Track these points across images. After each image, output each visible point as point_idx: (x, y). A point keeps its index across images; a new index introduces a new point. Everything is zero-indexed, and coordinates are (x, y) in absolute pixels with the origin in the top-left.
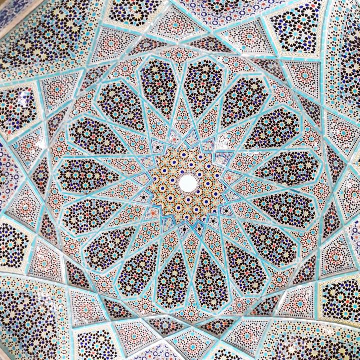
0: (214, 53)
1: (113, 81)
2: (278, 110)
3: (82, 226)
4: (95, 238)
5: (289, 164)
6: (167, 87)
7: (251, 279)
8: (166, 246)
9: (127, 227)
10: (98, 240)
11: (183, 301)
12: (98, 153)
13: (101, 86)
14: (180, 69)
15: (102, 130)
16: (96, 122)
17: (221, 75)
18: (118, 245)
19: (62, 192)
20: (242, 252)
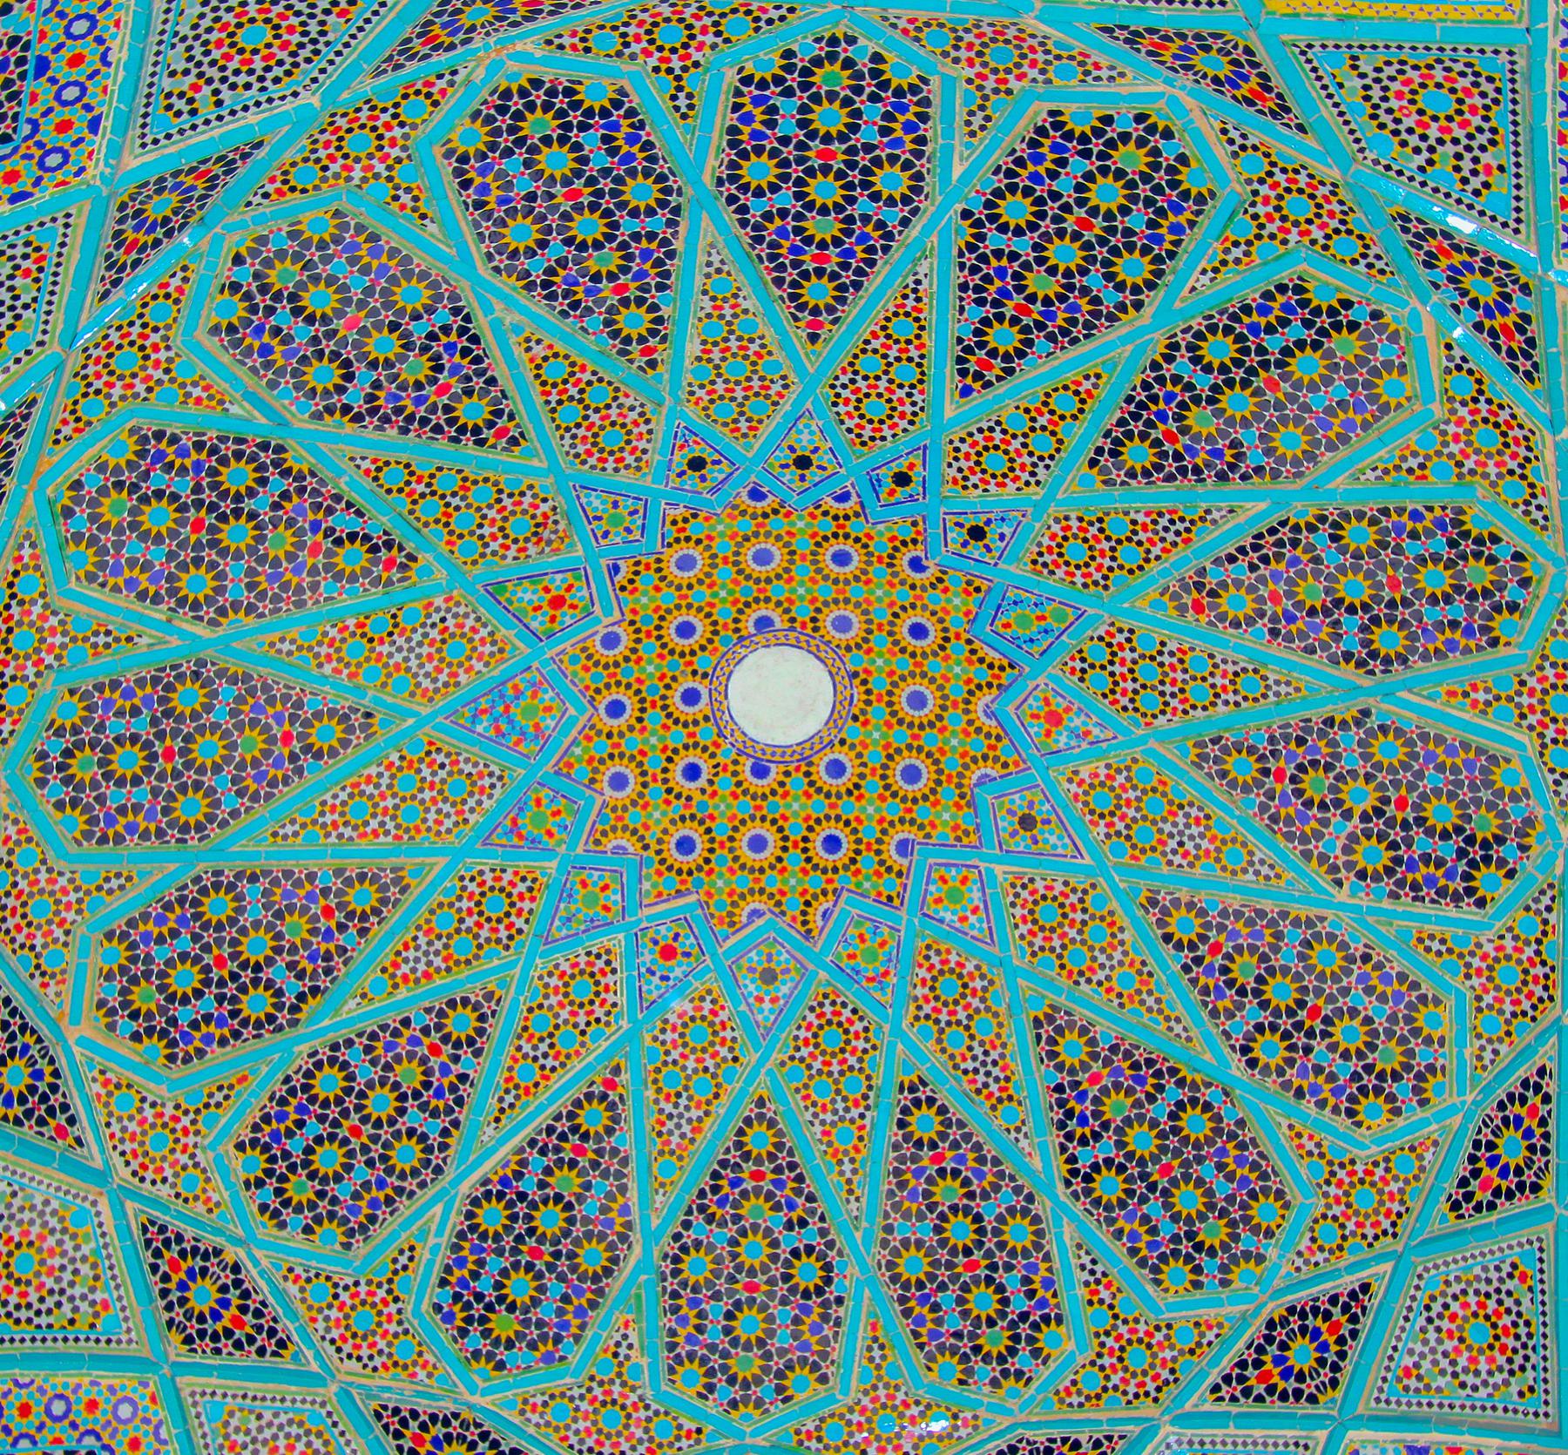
0: (219, 1241)
1: (694, 1414)
2: (103, 840)
3: (1383, 998)
4: (1386, 904)
5: (209, 555)
6: (513, 1218)
7: (829, 118)
8: (1129, 555)
9: (1216, 787)
10: (1387, 885)
11: (1282, 288)
12: (1018, 1190)
13: (755, 1433)
14: (403, 1260)
15: (914, 1265)
16: (907, 1313)
17: (256, 1128)
18: (1328, 767)
19: (1308, 1202)
20: (772, 258)
